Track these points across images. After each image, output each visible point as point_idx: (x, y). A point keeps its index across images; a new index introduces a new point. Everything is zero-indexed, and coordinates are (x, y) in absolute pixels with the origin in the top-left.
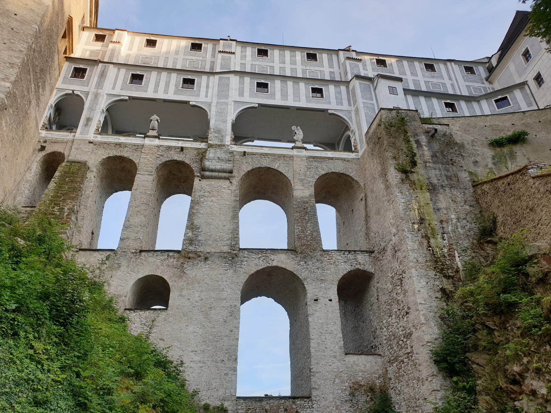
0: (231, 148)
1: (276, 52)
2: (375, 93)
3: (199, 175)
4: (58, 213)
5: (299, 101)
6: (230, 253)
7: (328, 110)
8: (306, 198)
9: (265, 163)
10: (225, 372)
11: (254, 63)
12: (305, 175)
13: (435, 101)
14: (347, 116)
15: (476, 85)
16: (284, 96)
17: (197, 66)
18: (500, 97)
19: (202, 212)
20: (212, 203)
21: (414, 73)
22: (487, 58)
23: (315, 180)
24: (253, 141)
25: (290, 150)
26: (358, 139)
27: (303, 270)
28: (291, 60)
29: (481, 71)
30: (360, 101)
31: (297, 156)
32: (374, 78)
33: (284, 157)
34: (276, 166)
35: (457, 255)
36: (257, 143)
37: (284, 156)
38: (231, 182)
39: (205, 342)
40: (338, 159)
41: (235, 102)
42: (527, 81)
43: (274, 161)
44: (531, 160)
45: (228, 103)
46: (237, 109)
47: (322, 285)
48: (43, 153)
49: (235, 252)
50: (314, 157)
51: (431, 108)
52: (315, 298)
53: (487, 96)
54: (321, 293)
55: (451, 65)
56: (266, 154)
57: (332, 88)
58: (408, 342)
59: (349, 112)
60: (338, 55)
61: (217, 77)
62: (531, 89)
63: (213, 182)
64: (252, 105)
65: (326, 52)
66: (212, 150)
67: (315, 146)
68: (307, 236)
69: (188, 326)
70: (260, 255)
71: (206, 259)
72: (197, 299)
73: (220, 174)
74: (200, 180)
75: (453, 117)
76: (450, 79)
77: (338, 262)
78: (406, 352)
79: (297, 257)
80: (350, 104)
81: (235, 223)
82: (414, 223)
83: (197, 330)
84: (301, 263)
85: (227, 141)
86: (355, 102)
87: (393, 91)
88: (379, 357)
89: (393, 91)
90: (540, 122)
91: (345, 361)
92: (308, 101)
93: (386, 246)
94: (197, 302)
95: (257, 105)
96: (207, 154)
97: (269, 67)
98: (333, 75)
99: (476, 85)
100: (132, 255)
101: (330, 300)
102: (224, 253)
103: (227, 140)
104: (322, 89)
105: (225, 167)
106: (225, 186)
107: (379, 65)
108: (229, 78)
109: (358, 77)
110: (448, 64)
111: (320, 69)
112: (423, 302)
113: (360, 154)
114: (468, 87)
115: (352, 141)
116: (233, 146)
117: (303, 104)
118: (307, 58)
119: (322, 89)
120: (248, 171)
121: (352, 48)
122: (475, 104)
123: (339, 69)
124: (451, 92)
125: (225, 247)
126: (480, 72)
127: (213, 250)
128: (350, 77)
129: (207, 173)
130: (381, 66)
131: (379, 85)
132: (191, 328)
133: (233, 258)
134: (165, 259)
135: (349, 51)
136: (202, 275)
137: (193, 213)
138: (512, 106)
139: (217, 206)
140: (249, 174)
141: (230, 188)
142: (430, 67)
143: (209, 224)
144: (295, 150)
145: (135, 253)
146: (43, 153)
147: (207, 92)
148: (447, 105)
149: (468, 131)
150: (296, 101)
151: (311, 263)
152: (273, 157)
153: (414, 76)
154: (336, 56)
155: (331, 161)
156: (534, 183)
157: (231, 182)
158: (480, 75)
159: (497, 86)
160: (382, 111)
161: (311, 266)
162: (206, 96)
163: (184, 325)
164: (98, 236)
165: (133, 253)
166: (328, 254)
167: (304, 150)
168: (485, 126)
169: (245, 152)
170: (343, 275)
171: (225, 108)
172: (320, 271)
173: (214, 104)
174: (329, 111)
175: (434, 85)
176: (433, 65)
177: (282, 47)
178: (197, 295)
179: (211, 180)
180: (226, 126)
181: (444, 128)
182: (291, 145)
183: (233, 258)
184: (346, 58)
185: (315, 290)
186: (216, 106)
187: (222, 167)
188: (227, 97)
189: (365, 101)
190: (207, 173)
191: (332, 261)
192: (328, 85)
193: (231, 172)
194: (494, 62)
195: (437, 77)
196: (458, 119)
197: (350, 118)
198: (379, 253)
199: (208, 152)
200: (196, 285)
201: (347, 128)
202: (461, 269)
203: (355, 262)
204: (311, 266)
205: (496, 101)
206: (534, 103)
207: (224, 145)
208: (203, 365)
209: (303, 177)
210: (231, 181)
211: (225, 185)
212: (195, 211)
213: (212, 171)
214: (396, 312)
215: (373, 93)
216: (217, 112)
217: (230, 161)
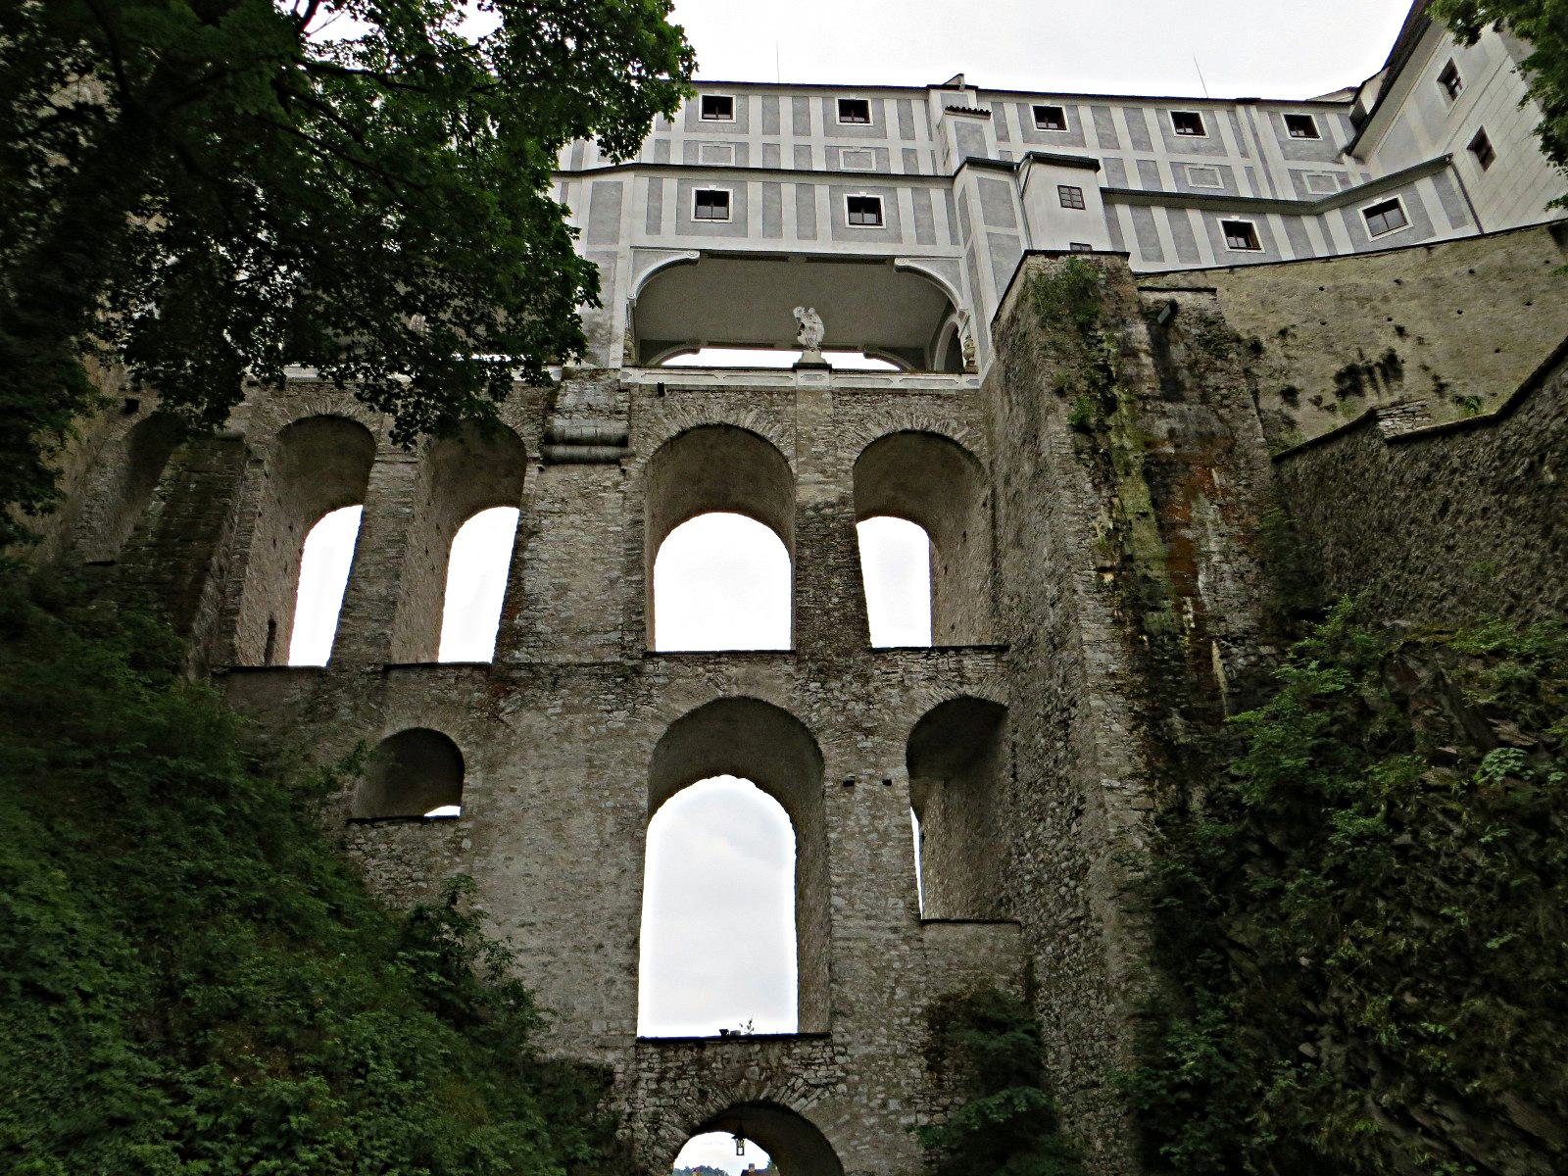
0: (626, 375)
1: (755, 102)
2: (1023, 205)
3: (537, 455)
4: (169, 577)
5: (814, 237)
6: (621, 664)
7: (893, 258)
8: (832, 506)
10: (608, 976)
11: (693, 136)
12: (828, 444)
13: (1195, 217)
14: (945, 273)
15: (1319, 167)
16: (773, 227)
18: (1378, 201)
19: (545, 556)
20: (572, 531)
21: (1141, 142)
22: (1350, 89)
24: (695, 351)
25: (790, 375)
26: (975, 336)
29: (1336, 129)
30: (980, 228)
32: (1018, 165)
35: (1216, 652)
36: (708, 357)
39: (553, 899)
40: (921, 393)
41: (637, 249)
42: (1450, 156)
44: (1443, 381)
45: (616, 253)
46: (641, 270)
48: (135, 420)
49: (631, 663)
50: (854, 392)
51: (1185, 241)
53: (1346, 200)
55: (1248, 112)
56: (722, 389)
57: (905, 193)
58: (1079, 890)
59: (952, 261)
60: (927, 101)
61: (588, 183)
62: (1463, 175)
63: (576, 473)
65: (894, 95)
66: (572, 386)
67: (868, 356)
69: (511, 859)
70: (700, 670)
72: (535, 789)
74: (541, 470)
76: (1244, 154)
77: (911, 679)
78: (1073, 916)
79: (800, 669)
80: (954, 240)
82: (1103, 570)
83: (535, 869)
85: (614, 359)
86: (968, 232)
87: (1071, 198)
88: (1015, 928)
89: (1071, 198)
90: (1472, 272)
91: (921, 940)
92: (837, 234)
93: (1035, 631)
94: (532, 796)
95: (697, 255)
96: (559, 398)
97: (733, 147)
99: (1319, 167)
102: (604, 665)
103: (612, 355)
104: (877, 201)
105: (606, 431)
106: (608, 483)
107: (1044, 125)
109: (973, 163)
110: (1240, 110)
111: (878, 143)
112: (1117, 784)
113: (981, 377)
114: (1295, 175)
115: (963, 341)
116: (630, 371)
118: (841, 115)
119: (877, 201)
121: (968, 81)
122: (1309, 224)
124: (1246, 192)
126: (1329, 132)
128: (955, 162)
129: (560, 451)
130: (1051, 125)
131: (1032, 182)
132: (518, 866)
133: (627, 679)
135: (956, 88)
136: (545, 725)
138: (1411, 225)
140: (671, 444)
141: (621, 488)
142: (1187, 122)
144: (801, 373)
145: (374, 672)
146: (135, 420)
148: (1232, 229)
149: (1274, 303)
150: (806, 238)
155: (898, 400)
156: (1391, 459)
158: (1330, 138)
159: (1378, 169)
160: (1031, 260)
161: (836, 693)
163: (502, 856)
164: (290, 626)
165: (368, 674)
166: (885, 659)
167: (826, 374)
168: (1322, 289)
169: (661, 387)
170: (922, 713)
172: (861, 706)
174: (898, 262)
175: (1200, 172)
176: (1197, 115)
177: (772, 89)
178: (533, 779)
179: (570, 467)
180: (611, 318)
181: (1204, 299)
182: (787, 358)
184: (947, 109)
187: (599, 430)
188: (614, 239)
189: (993, 229)
190: (560, 451)
191: (895, 678)
192: (895, 189)
193: (623, 442)
194: (1368, 102)
195: (1209, 151)
196: (1246, 272)
197: (956, 279)
198: (1020, 650)
199: (562, 392)
200: (531, 752)
201: (950, 307)
202: (1224, 688)
204: (836, 693)
205: (1369, 213)
206: (1469, 217)
207: (604, 370)
208: (550, 958)
214: (1053, 810)
217: (620, 413)
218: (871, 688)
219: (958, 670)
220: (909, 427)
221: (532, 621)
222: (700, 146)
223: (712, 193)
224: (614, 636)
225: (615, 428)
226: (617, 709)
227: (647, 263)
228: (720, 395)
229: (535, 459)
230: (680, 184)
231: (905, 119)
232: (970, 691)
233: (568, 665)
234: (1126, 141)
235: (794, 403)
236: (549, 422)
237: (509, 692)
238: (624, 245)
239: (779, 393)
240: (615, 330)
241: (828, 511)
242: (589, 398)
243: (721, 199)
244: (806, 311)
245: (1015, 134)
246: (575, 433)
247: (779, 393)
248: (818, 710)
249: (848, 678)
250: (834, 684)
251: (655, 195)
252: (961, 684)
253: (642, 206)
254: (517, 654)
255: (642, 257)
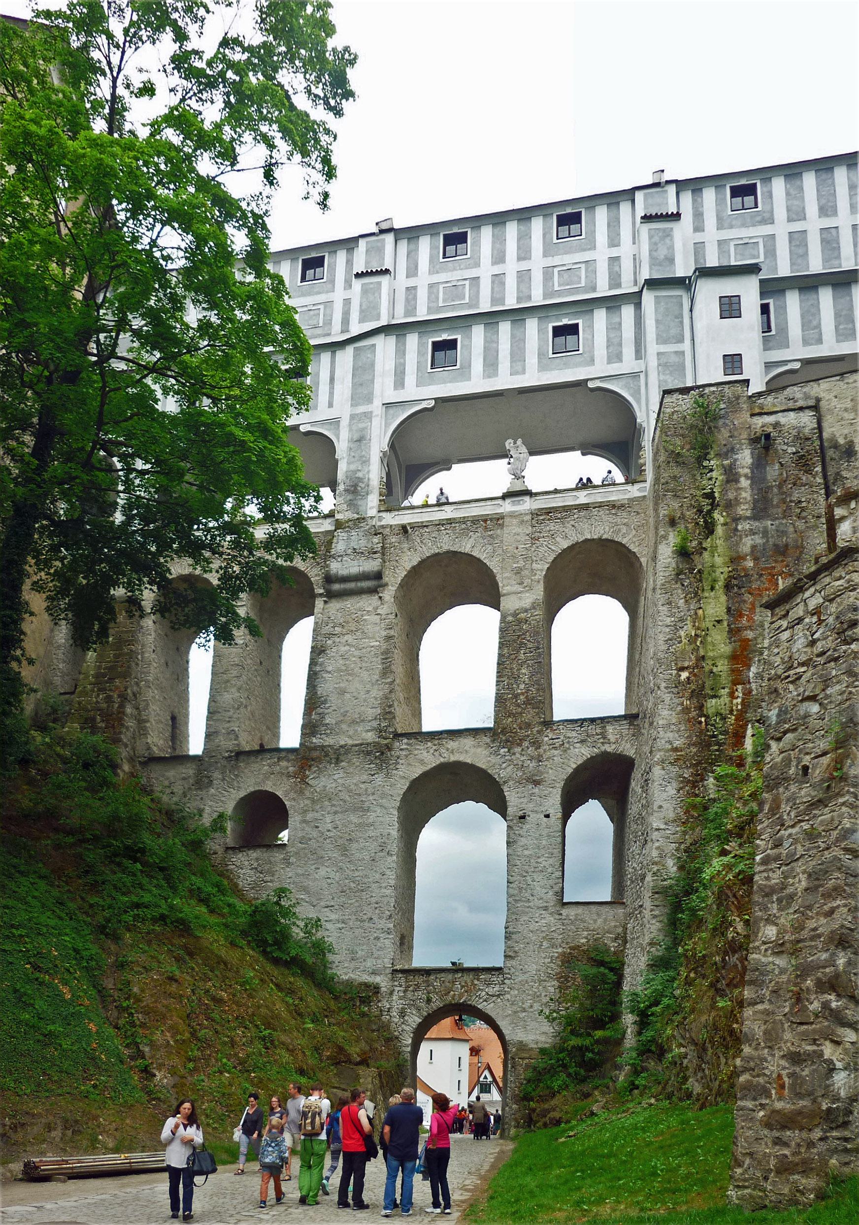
0: (380, 519)
3: (321, 591)
6: (378, 743)
8: (526, 611)
9: (446, 543)
11: (436, 278)
12: (526, 558)
17: (315, 322)
19: (330, 669)
20: (347, 648)
23: (547, 566)
25: (500, 502)
27: (504, 765)
28: (519, 248)
31: (512, 515)
33: (485, 521)
34: (469, 546)
37: (485, 519)
38: (380, 598)
40: (600, 505)
41: (388, 405)
43: (465, 533)
45: (371, 412)
47: (534, 791)
49: (386, 742)
50: (548, 511)
52: (521, 813)
54: (531, 805)
60: (633, 201)
61: (350, 350)
64: (424, 405)
66: (341, 535)
68: (516, 696)
71: (338, 761)
73: (359, 584)
74: (325, 602)
75: (842, 374)
77: (568, 742)
81: (387, 684)
84: (502, 750)
85: (371, 508)
98: (617, 269)
100: (224, 762)
101: (547, 816)
103: (370, 504)
105: (366, 569)
106: (370, 609)
108: (374, 345)
111: (587, 256)
116: (384, 514)
117: (532, 378)
120: (414, 568)
123: (634, 243)
125: (370, 734)
127: (350, 742)
129: (336, 587)
133: (382, 753)
134: (275, 763)
137: (316, 673)
139: (357, 653)
141: (379, 611)
143: (342, 692)
144: (508, 501)
147: (331, 394)
151: (519, 749)
152: (463, 526)
153: (827, 216)
154: (629, 204)
157: (380, 598)
161: (518, 755)
162: (330, 405)
169: (404, 529)
170: (574, 766)
171: (366, 428)
172: (533, 764)
173: (345, 423)
177: (498, 219)
180: (368, 472)
183: (382, 753)
185: (522, 800)
186: (350, 425)
187: (361, 569)
188: (369, 399)
190: (336, 587)
193: (378, 576)
199: (335, 540)
203: (602, 740)
204: (518, 755)
207: (364, 519)
209: (521, 564)
210: (381, 595)
211: (370, 604)
212: (318, 668)
213: (345, 579)
215: (686, 321)
216: (351, 440)
217: (375, 553)
218: (541, 751)
219: (601, 734)
220: (589, 537)
221: (322, 716)
222: (441, 287)
223: (445, 341)
224: (375, 724)
225: (371, 565)
226: (378, 773)
227: (394, 417)
228: (448, 526)
229: (321, 595)
230: (420, 337)
231: (614, 225)
232: (609, 748)
233: (346, 745)
234: (812, 208)
235: (502, 526)
236: (328, 566)
237: (310, 766)
238: (377, 403)
239: (491, 520)
240: (371, 483)
241: (523, 615)
242: (354, 544)
243: (451, 345)
244: (515, 443)
245: (710, 220)
246: (344, 572)
247: (491, 520)
248: (505, 768)
249: (526, 744)
250: (518, 750)
251: (401, 352)
252: (603, 743)
253: (390, 365)
254: (314, 740)
255: (391, 411)
